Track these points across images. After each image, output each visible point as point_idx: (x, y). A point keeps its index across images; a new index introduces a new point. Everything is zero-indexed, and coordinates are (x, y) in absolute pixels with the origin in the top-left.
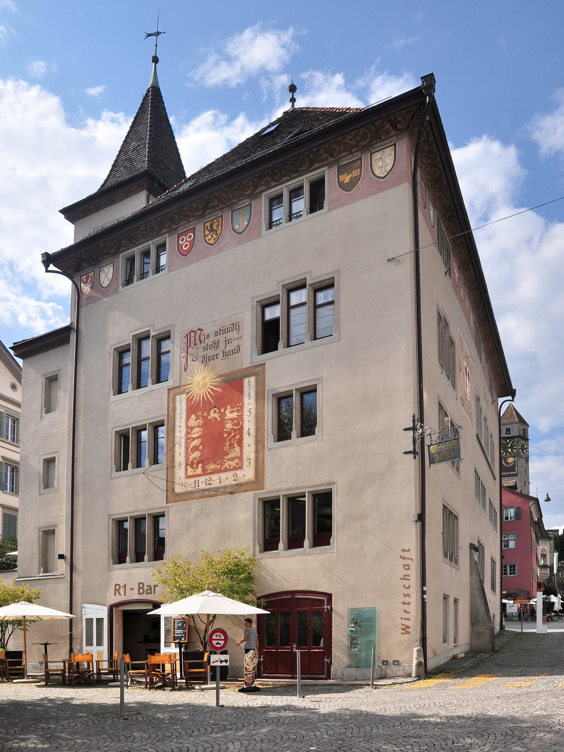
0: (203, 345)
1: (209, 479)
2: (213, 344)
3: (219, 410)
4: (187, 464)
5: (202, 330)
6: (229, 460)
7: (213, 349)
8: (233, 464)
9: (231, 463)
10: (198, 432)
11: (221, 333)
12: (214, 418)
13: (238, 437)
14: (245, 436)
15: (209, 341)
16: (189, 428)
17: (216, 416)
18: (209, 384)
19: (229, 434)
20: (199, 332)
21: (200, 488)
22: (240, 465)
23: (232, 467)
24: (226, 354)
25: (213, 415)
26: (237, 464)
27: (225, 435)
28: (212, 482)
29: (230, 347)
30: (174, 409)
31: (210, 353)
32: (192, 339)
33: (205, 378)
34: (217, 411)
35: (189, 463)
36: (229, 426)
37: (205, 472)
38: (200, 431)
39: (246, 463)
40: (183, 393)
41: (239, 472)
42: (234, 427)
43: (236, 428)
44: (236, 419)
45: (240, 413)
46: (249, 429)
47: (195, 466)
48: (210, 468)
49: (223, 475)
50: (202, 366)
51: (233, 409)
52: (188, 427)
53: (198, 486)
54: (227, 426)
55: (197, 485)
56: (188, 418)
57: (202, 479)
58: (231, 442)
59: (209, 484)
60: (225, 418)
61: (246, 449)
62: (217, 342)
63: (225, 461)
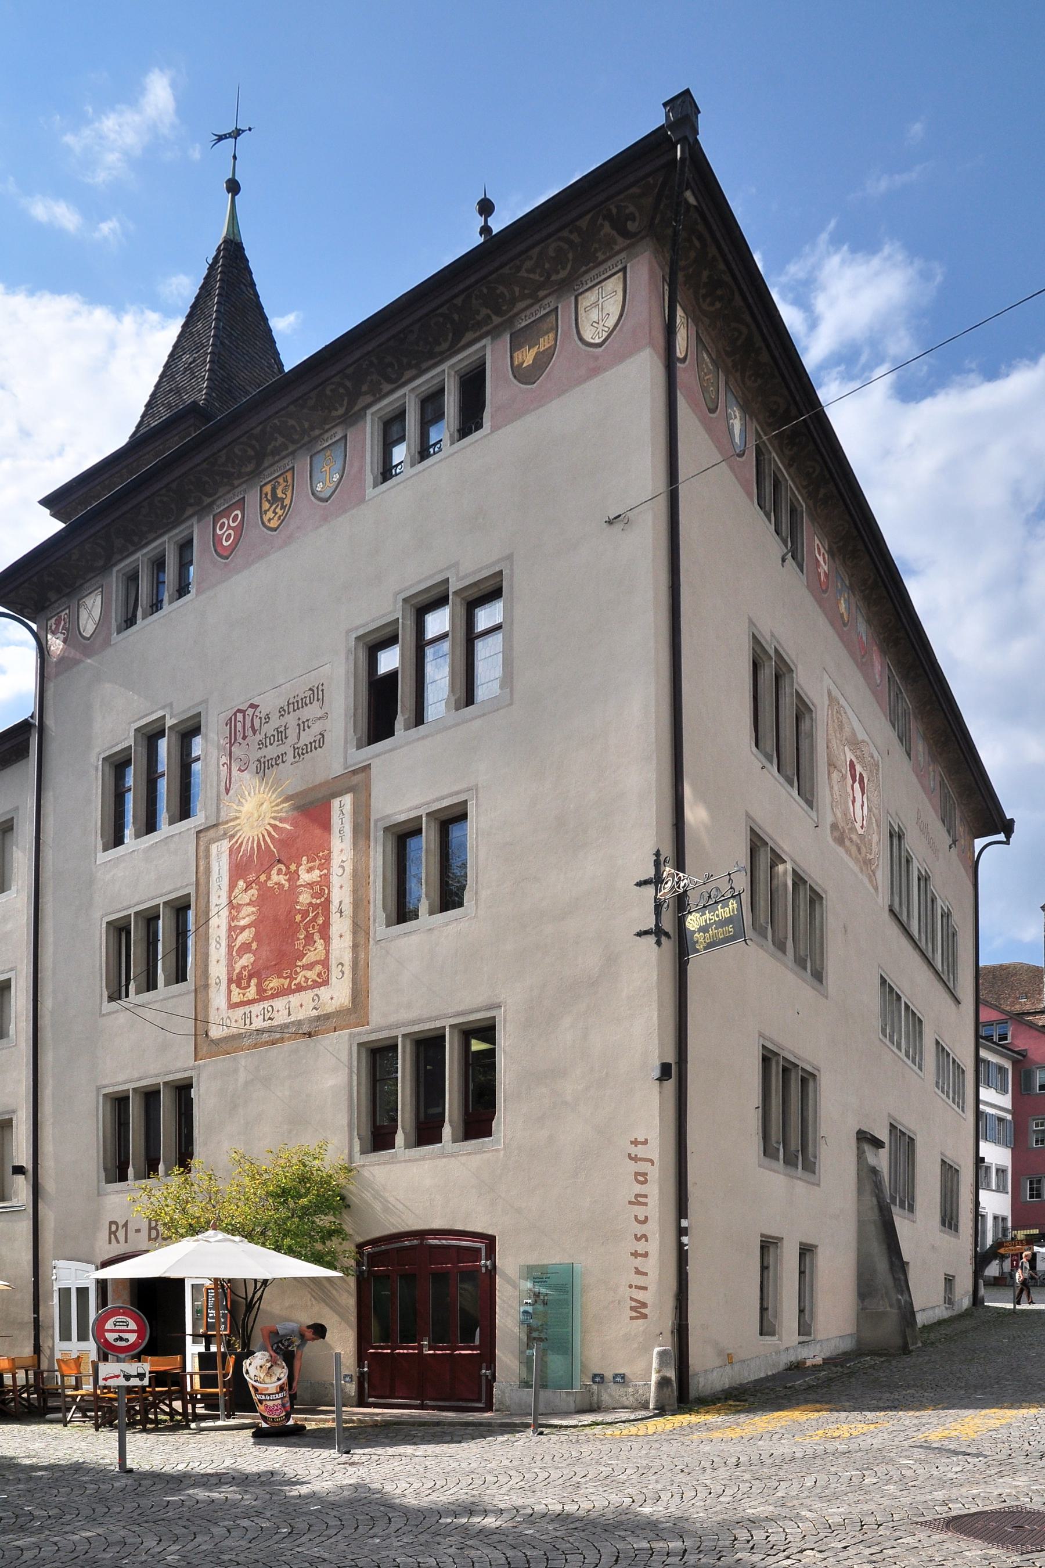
0: (259, 737)
1: (270, 1009)
2: (275, 733)
3: (288, 868)
4: (230, 981)
6: (303, 967)
7: (276, 743)
11: (291, 709)
13: (320, 920)
14: (334, 917)
15: (269, 729)
16: (233, 908)
17: (282, 879)
18: (269, 815)
19: (305, 914)
20: (250, 711)
21: (253, 1027)
23: (310, 983)
24: (300, 753)
25: (277, 878)
27: (298, 918)
28: (275, 1015)
29: (306, 738)
31: (271, 752)
32: (239, 726)
34: (284, 868)
35: (235, 977)
36: (305, 898)
37: (262, 996)
39: (335, 972)
42: (314, 901)
44: (318, 883)
45: (325, 871)
46: (341, 903)
47: (244, 983)
48: (271, 985)
49: (295, 999)
54: (301, 899)
55: (248, 1021)
56: (232, 886)
57: (256, 1009)
58: (307, 932)
59: (270, 1019)
62: (282, 729)
63: (298, 969)
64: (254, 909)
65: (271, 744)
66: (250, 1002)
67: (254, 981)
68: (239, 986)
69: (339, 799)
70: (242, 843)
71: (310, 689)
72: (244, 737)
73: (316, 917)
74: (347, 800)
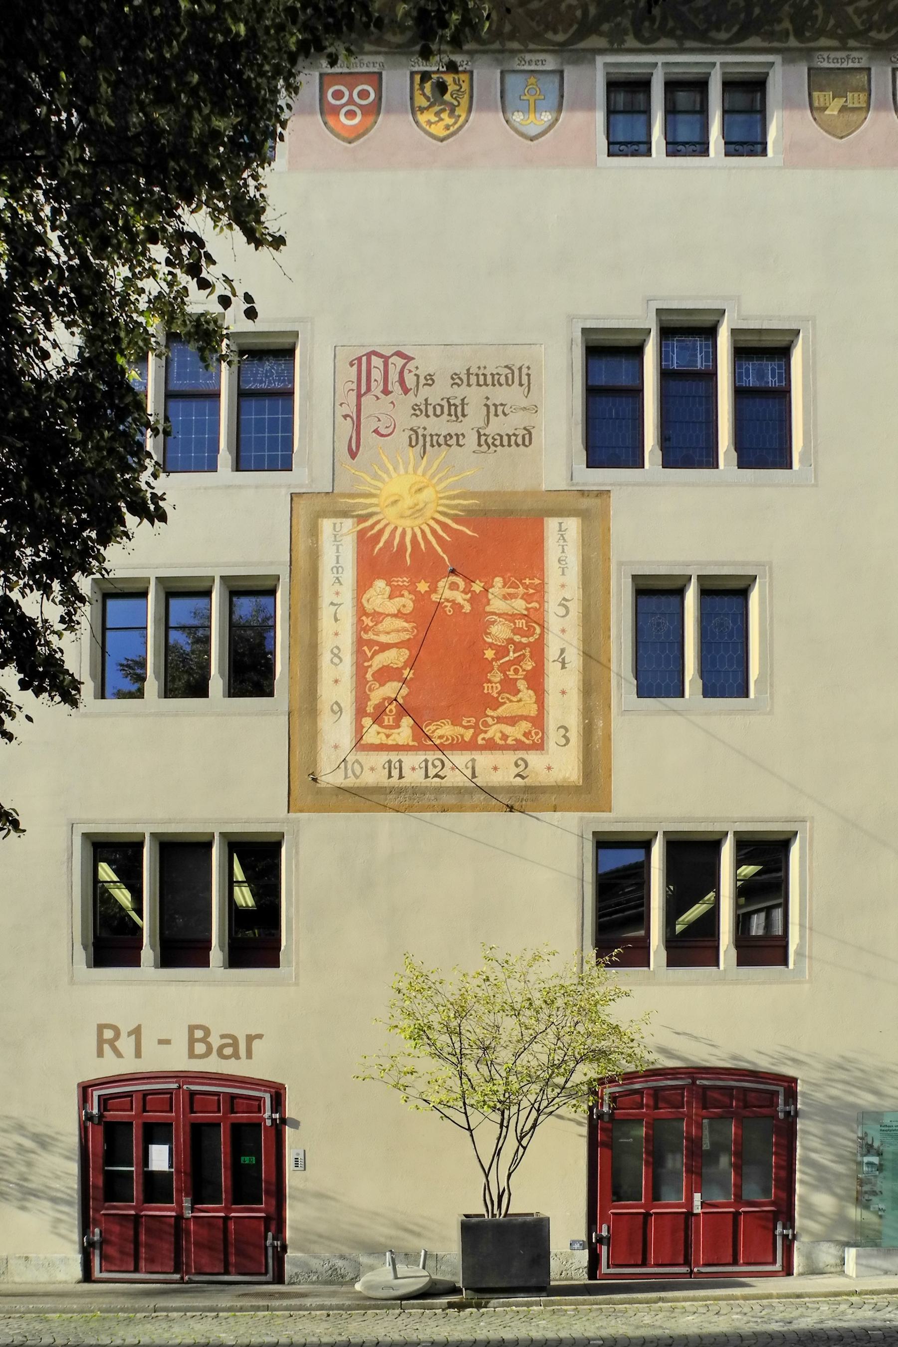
0: (411, 399)
1: (438, 763)
2: (445, 403)
4: (360, 712)
5: (409, 359)
6: (500, 720)
8: (515, 732)
9: (508, 730)
10: (398, 631)
11: (473, 379)
12: (453, 601)
13: (529, 665)
14: (552, 669)
16: (367, 615)
17: (460, 597)
19: (502, 651)
20: (400, 362)
22: (536, 738)
25: (451, 593)
26: (527, 735)
27: (489, 654)
28: (446, 772)
30: (314, 555)
32: (377, 375)
33: (420, 490)
35: (370, 709)
36: (500, 631)
37: (422, 741)
38: (405, 630)
39: (553, 736)
40: (345, 514)
41: (534, 759)
42: (517, 638)
43: (524, 640)
46: (563, 651)
47: (388, 720)
48: (440, 732)
49: (484, 760)
50: (412, 454)
51: (512, 590)
52: (361, 611)
53: (401, 777)
54: (494, 629)
55: (395, 773)
57: (412, 760)
59: (436, 776)
60: (488, 609)
61: (552, 699)
63: (489, 720)
64: (406, 625)
65: (438, 416)
66: (397, 748)
67: (407, 722)
68: (377, 719)
69: (560, 520)
70: (381, 532)
71: (506, 367)
72: (386, 392)
73: (518, 660)
74: (573, 525)
